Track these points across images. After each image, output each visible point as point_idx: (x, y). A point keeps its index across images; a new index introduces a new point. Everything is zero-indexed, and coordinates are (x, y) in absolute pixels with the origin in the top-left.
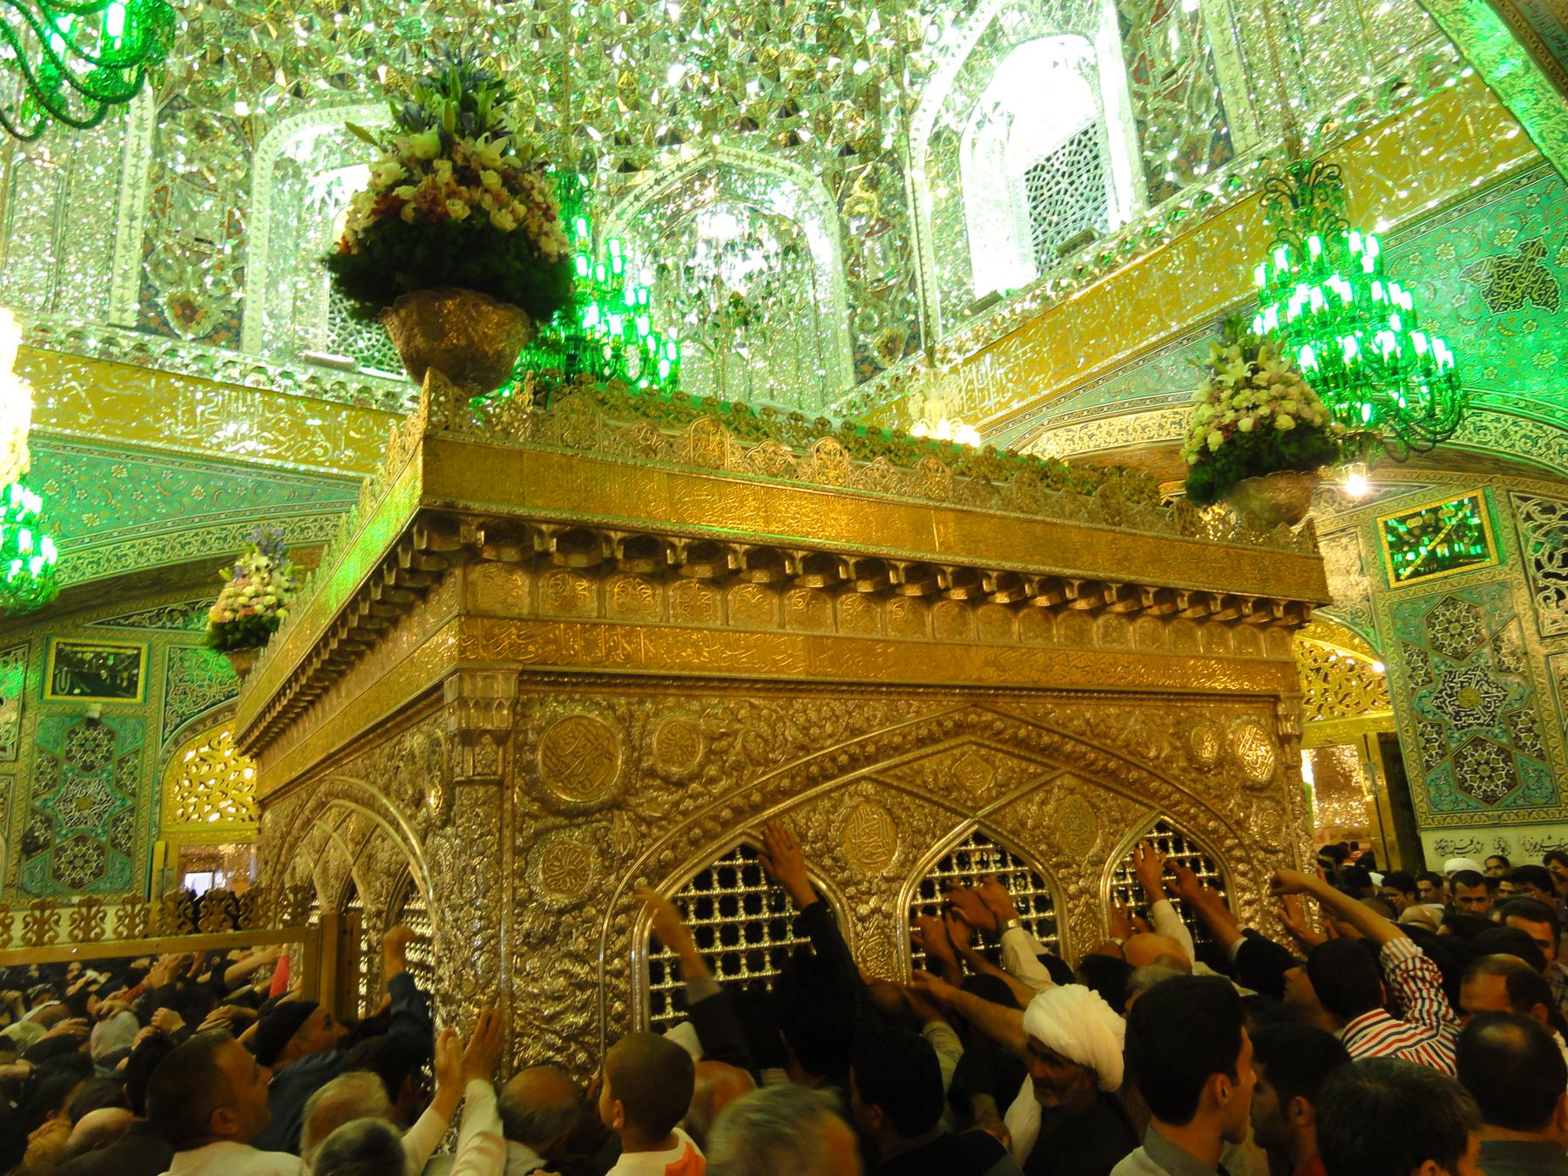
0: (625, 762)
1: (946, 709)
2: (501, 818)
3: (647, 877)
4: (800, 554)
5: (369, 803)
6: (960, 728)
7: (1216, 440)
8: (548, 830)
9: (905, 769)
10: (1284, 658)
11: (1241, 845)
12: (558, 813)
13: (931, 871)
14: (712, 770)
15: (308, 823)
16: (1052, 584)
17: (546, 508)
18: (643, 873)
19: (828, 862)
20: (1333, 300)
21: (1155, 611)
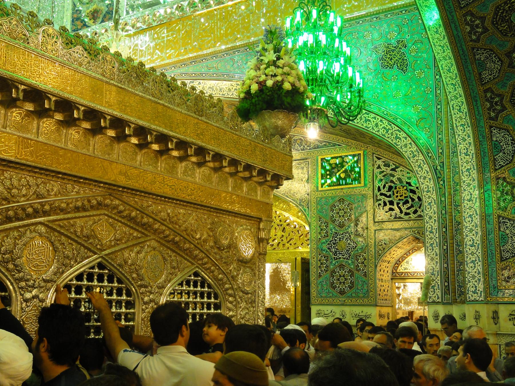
1: (96, 194)
6: (100, 205)
7: (255, 87)
9: (65, 222)
10: (267, 201)
11: (232, 288)
13: (71, 280)
16: (162, 138)
20: (317, 42)
21: (211, 165)
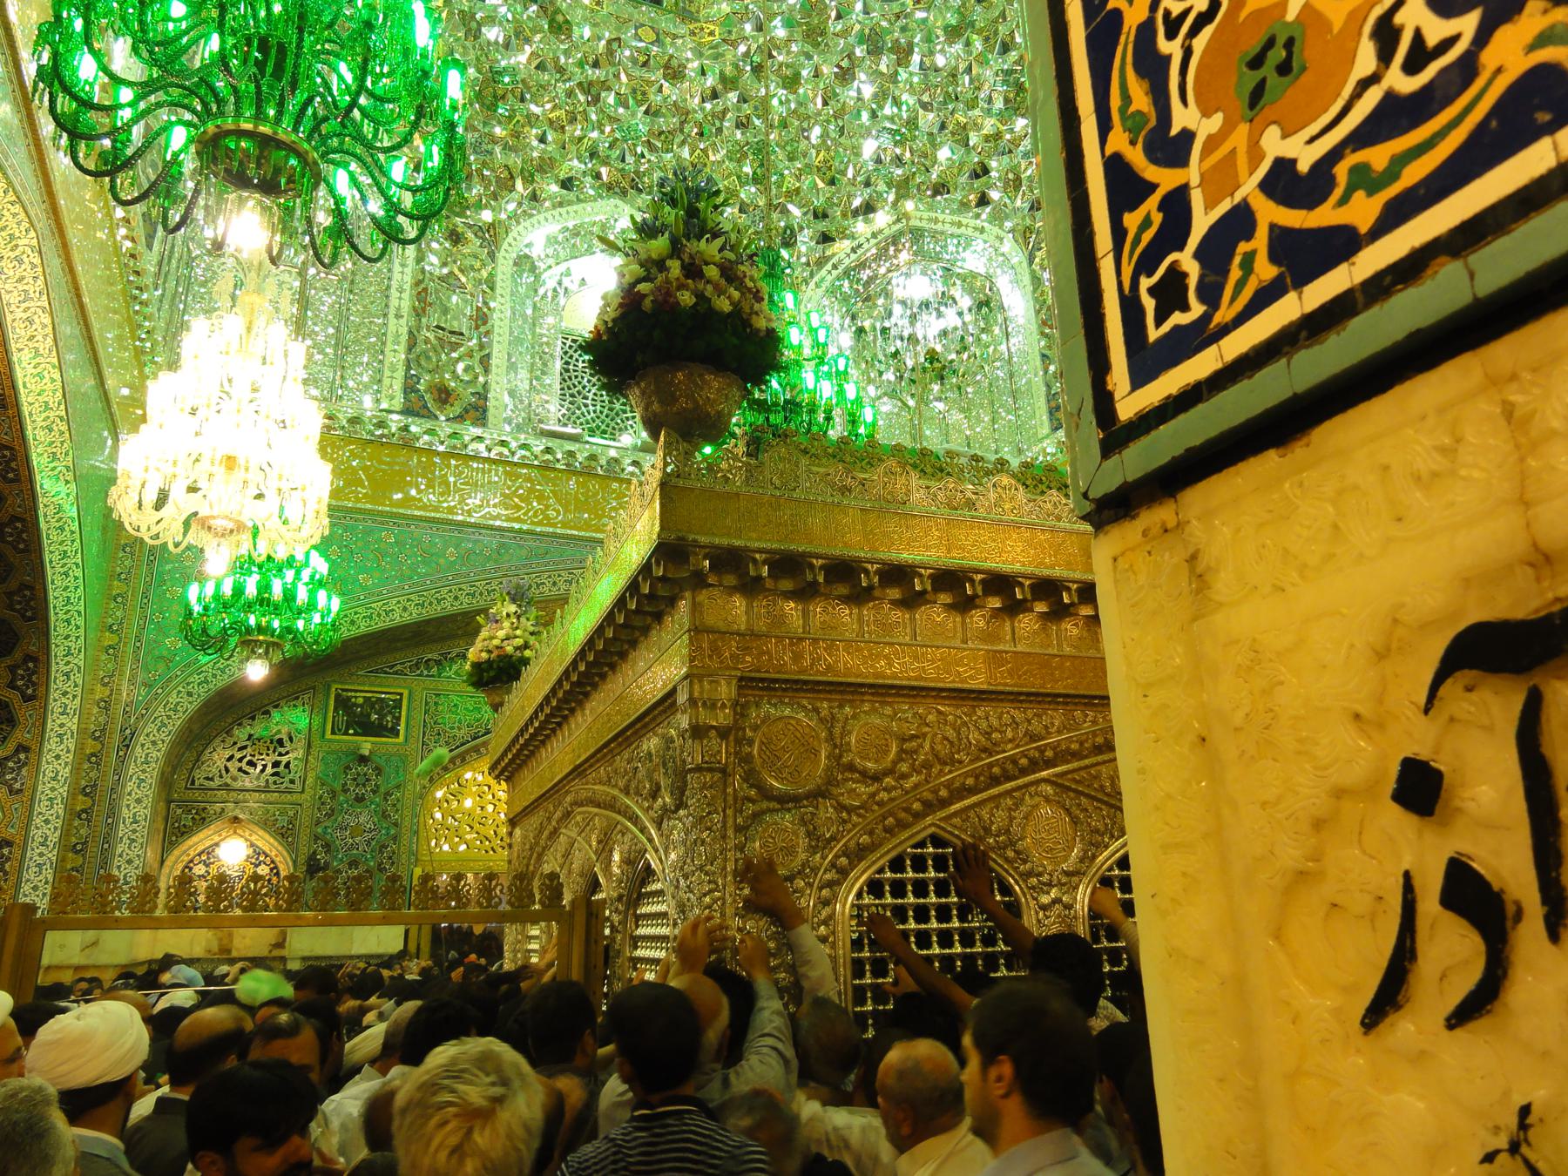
0: (828, 758)
2: (725, 800)
4: (980, 577)
5: (611, 805)
8: (764, 812)
13: (1110, 869)
14: (904, 768)
15: (555, 833)
17: (760, 540)
18: (845, 853)
19: (1010, 854)
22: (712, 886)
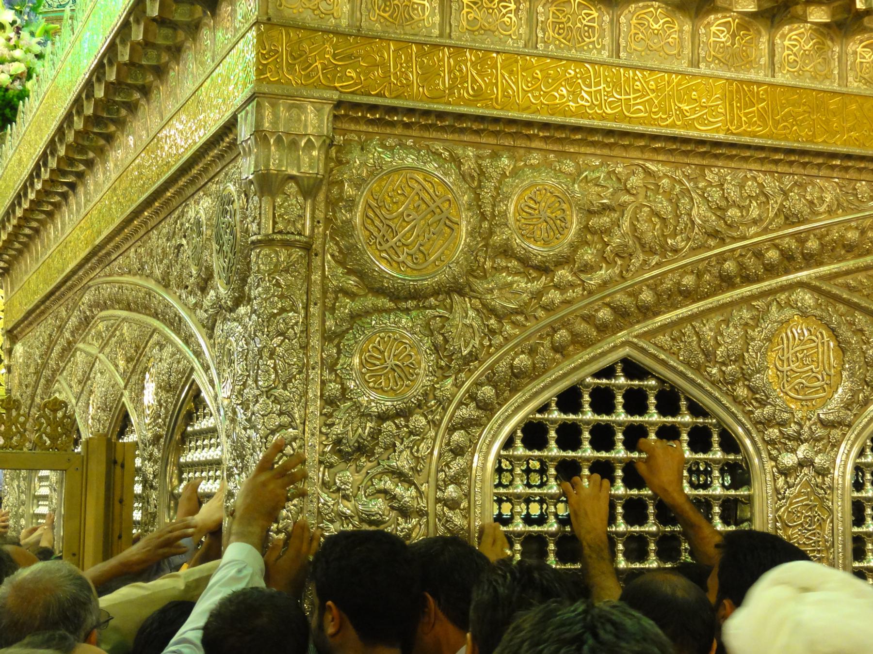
0: (470, 234)
3: (495, 387)
5: (143, 305)
12: (380, 291)
14: (588, 255)
15: (69, 349)
19: (742, 391)
22: (285, 419)
